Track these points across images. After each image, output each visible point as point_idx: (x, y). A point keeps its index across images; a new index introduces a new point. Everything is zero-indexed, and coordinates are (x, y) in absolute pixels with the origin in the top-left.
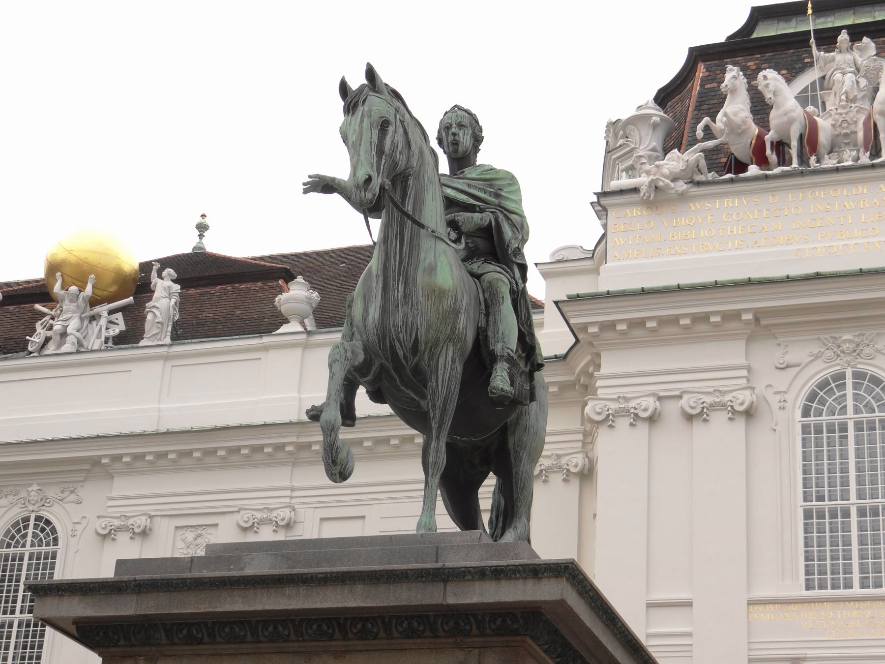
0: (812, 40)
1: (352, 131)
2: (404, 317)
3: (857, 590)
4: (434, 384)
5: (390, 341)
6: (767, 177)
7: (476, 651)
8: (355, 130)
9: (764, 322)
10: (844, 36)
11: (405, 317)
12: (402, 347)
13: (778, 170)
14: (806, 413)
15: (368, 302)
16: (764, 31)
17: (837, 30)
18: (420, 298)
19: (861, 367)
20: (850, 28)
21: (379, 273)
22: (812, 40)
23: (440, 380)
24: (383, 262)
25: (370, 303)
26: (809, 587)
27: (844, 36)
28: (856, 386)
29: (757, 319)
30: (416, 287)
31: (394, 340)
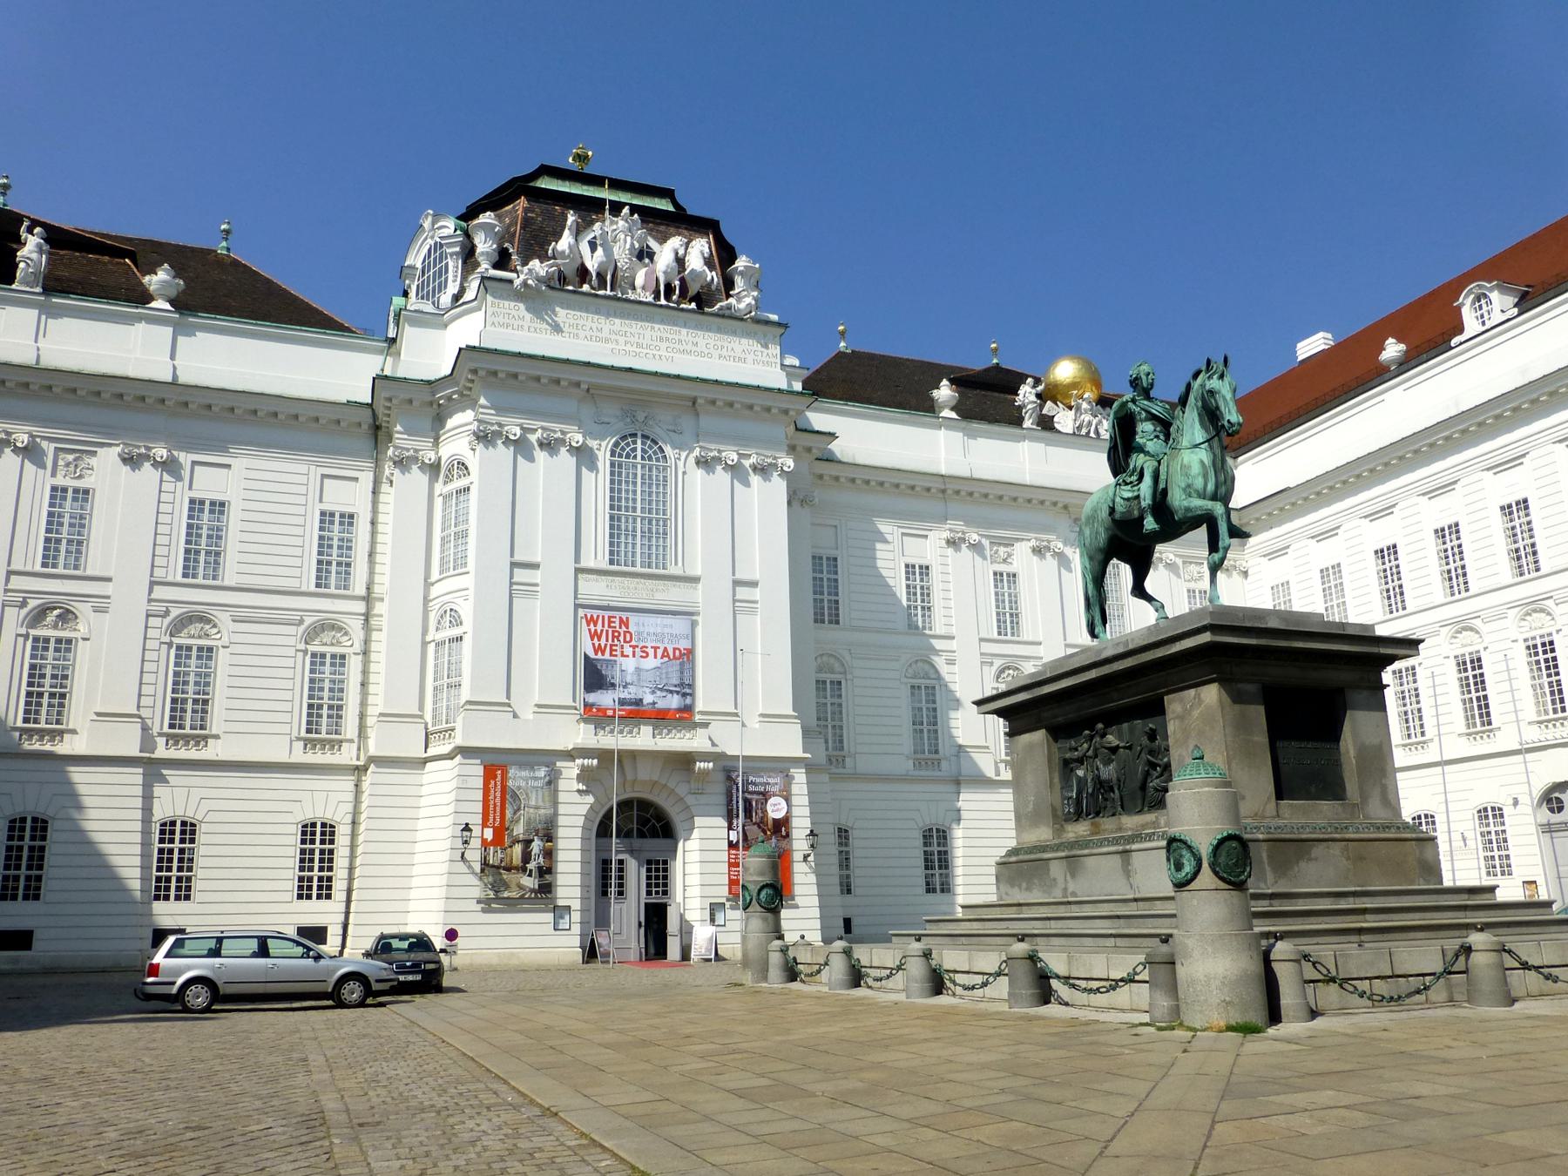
0: (607, 207)
3: (638, 569)
6: (597, 296)
9: (591, 391)
10: (626, 210)
13: (601, 292)
14: (613, 454)
16: (546, 183)
17: (625, 204)
19: (646, 433)
20: (631, 205)
22: (607, 207)
26: (611, 562)
27: (626, 210)
28: (643, 443)
29: (588, 390)
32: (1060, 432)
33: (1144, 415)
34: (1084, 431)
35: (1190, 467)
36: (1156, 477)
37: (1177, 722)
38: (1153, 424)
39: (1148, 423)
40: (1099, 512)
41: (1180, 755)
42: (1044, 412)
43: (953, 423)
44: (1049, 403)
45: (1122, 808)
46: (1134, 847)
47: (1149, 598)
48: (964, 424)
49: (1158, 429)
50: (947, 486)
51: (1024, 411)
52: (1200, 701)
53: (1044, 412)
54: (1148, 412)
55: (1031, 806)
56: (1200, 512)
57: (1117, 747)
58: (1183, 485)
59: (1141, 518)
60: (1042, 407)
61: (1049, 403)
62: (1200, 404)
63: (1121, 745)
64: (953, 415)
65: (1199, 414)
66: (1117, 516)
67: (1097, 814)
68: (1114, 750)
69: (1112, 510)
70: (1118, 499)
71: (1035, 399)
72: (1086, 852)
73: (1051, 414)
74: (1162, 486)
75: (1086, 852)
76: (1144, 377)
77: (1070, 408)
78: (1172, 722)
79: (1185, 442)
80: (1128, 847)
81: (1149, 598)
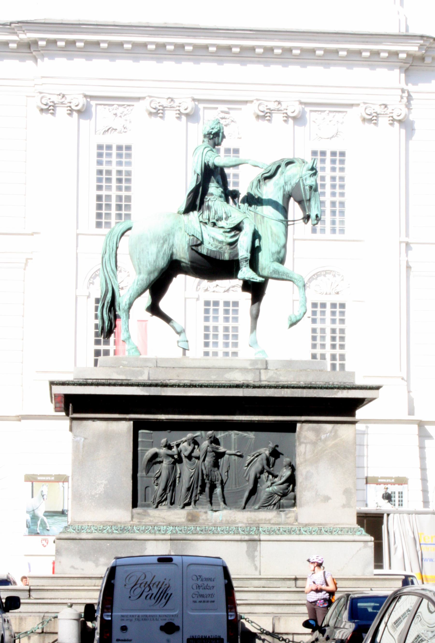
35: (278, 237)
36: (256, 235)
37: (309, 446)
40: (171, 237)
41: (308, 472)
45: (225, 502)
52: (336, 436)
55: (101, 489)
63: (228, 452)
65: (284, 195)
66: (204, 252)
67: (188, 504)
72: (200, 537)
75: (200, 537)
78: (303, 446)
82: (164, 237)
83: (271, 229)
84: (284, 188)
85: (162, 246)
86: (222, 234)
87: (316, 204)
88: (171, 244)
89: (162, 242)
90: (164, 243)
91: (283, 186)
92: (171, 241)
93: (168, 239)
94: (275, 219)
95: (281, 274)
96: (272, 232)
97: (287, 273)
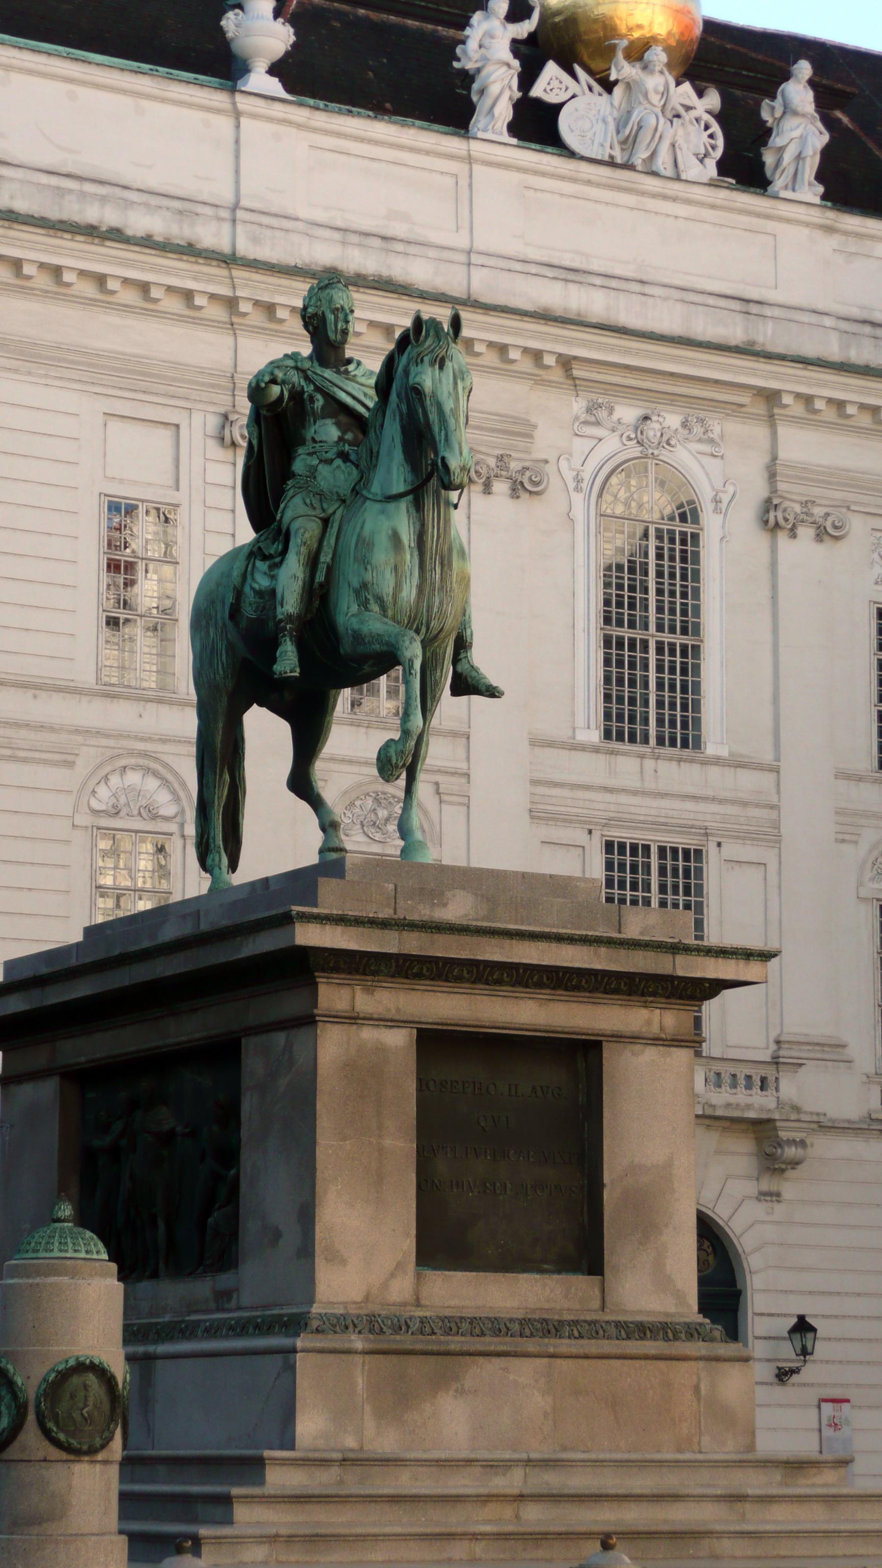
1: (445, 394)
2: (440, 603)
4: (438, 674)
5: (418, 625)
7: (658, 1011)
8: (449, 393)
11: (441, 603)
12: (427, 632)
15: (401, 576)
18: (454, 585)
21: (412, 545)
23: (444, 670)
24: (417, 532)
25: (404, 578)
30: (451, 570)
31: (422, 624)
32: (572, 154)
33: (320, 402)
34: (641, 155)
38: (338, 425)
39: (329, 422)
40: (219, 606)
42: (537, 91)
43: (278, 110)
44: (551, 69)
46: (162, 1348)
47: (315, 801)
48: (300, 114)
49: (349, 436)
50: (239, 293)
51: (475, 86)
53: (537, 91)
54: (330, 398)
56: (377, 647)
57: (172, 1133)
58: (355, 583)
59: (274, 644)
60: (527, 78)
61: (551, 69)
62: (404, 407)
64: (274, 86)
65: (403, 428)
68: (168, 1138)
69: (235, 612)
70: (247, 589)
71: (508, 56)
73: (552, 98)
74: (320, 577)
76: (330, 317)
77: (608, 86)
79: (376, 488)
80: (151, 1349)
81: (315, 801)
82: (205, 610)
83: (362, 527)
84: (399, 409)
85: (208, 633)
86: (265, 573)
87: (443, 433)
88: (220, 623)
89: (204, 623)
90: (208, 626)
91: (398, 406)
92: (219, 617)
93: (213, 613)
94: (379, 498)
95: (366, 640)
96: (359, 535)
97: (378, 635)
